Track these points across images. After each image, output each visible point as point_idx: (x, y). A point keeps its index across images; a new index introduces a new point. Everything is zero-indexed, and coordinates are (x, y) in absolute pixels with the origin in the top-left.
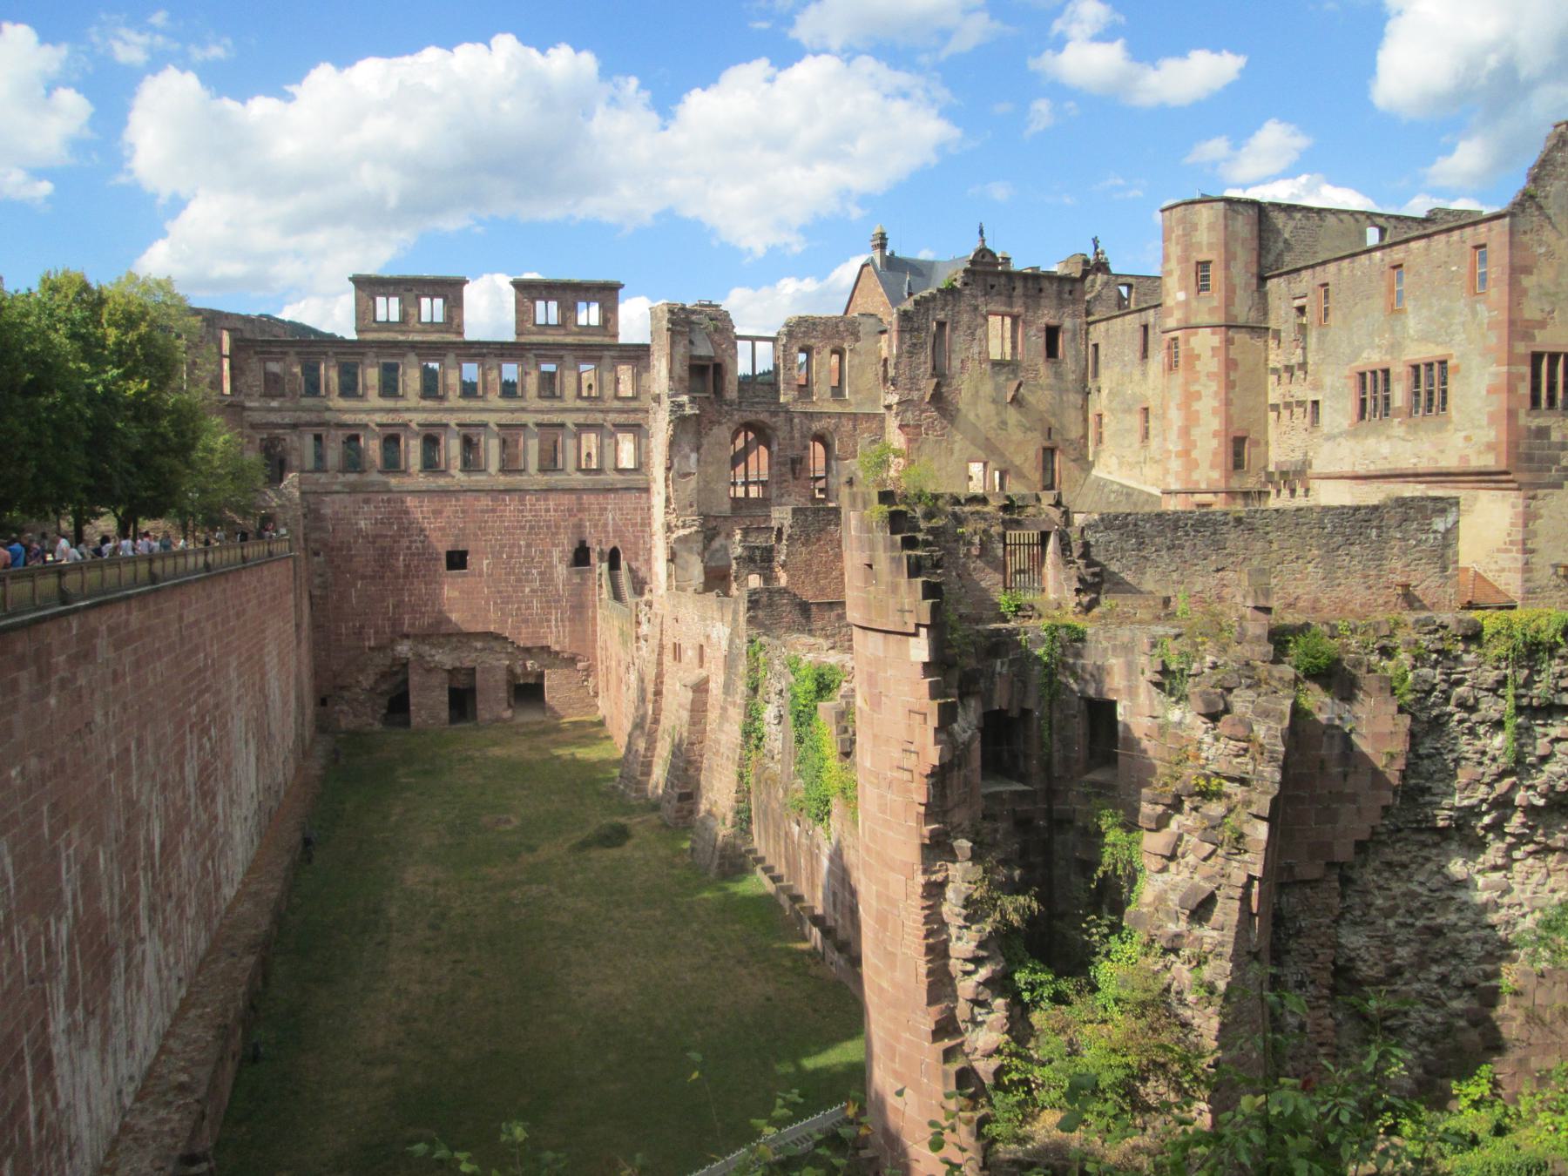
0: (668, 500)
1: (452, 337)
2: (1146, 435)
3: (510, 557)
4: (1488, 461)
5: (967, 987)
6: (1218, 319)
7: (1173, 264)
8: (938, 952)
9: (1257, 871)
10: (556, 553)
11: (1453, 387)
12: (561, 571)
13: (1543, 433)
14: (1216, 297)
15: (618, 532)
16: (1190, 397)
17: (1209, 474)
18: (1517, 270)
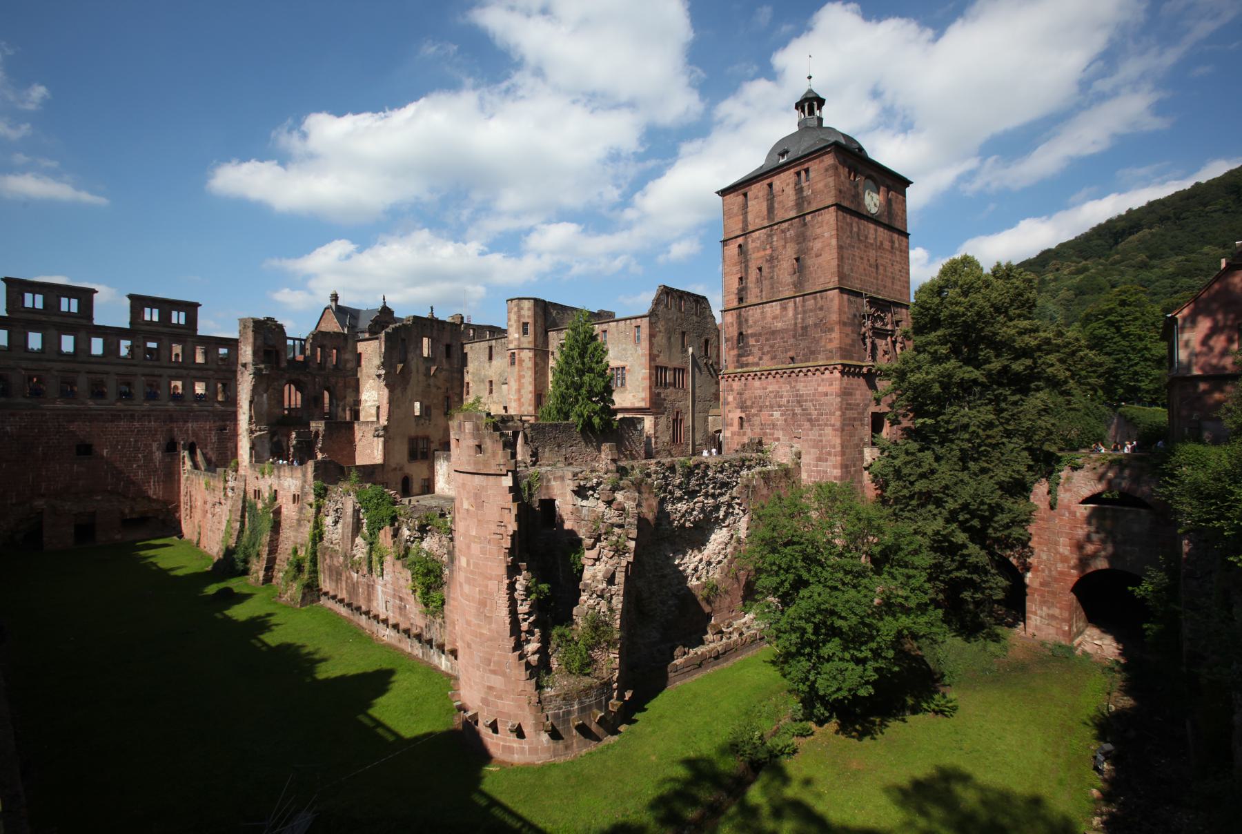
0: (251, 418)
1: (84, 322)
2: (491, 392)
3: (123, 447)
4: (642, 405)
5: (524, 626)
6: (531, 346)
7: (512, 322)
8: (513, 613)
9: (631, 559)
10: (155, 446)
11: (628, 377)
12: (158, 455)
13: (659, 394)
14: (530, 337)
15: (195, 434)
16: (521, 377)
17: (528, 408)
18: (652, 336)
